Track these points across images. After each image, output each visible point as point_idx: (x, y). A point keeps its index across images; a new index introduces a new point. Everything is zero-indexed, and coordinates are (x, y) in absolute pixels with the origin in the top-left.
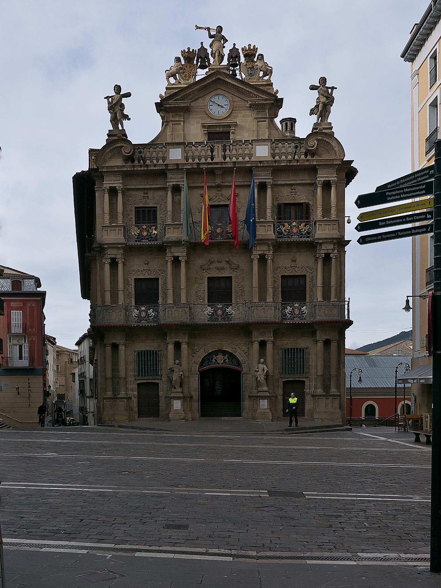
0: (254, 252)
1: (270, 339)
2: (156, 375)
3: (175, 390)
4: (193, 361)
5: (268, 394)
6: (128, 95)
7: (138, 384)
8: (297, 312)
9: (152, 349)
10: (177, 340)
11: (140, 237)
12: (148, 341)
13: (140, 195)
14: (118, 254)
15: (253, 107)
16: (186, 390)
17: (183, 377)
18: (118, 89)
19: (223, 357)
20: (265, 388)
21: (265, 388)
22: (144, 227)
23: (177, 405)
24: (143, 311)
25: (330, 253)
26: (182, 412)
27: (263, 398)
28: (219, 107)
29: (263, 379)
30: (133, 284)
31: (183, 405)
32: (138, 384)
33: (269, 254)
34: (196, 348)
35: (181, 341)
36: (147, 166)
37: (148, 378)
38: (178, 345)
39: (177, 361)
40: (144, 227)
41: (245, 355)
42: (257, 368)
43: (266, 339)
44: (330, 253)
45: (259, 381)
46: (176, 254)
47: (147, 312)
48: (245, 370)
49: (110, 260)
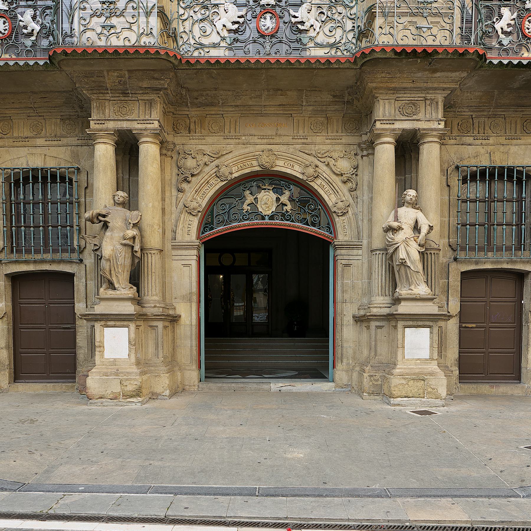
1: (434, 125)
3: (110, 293)
4: (181, 205)
5: (431, 308)
9: (51, 164)
12: (40, 142)
16: (152, 296)
17: (137, 248)
19: (274, 196)
20: (422, 290)
21: (422, 290)
23: (116, 343)
26: (134, 369)
27: (417, 320)
29: (416, 256)
31: (135, 344)
34: (190, 163)
37: (39, 257)
38: (127, 149)
39: (122, 195)
41: (344, 189)
42: (392, 217)
45: (403, 263)
48: (343, 235)
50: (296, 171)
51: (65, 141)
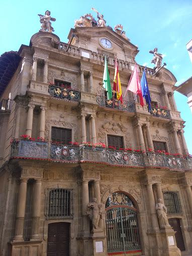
0: (139, 121)
2: (69, 215)
6: (54, 20)
7: (50, 225)
8: (174, 163)
9: (65, 187)
10: (92, 179)
11: (61, 96)
12: (61, 180)
13: (59, 72)
14: (43, 104)
15: (123, 50)
18: (48, 13)
22: (65, 90)
24: (65, 149)
25: (180, 130)
28: (106, 44)
30: (50, 130)
32: (50, 225)
33: (148, 124)
35: (95, 180)
36: (69, 54)
40: (65, 90)
43: (157, 182)
44: (180, 130)
46: (89, 113)
47: (68, 151)
49: (34, 106)
50: (127, 191)
51: (68, 180)
